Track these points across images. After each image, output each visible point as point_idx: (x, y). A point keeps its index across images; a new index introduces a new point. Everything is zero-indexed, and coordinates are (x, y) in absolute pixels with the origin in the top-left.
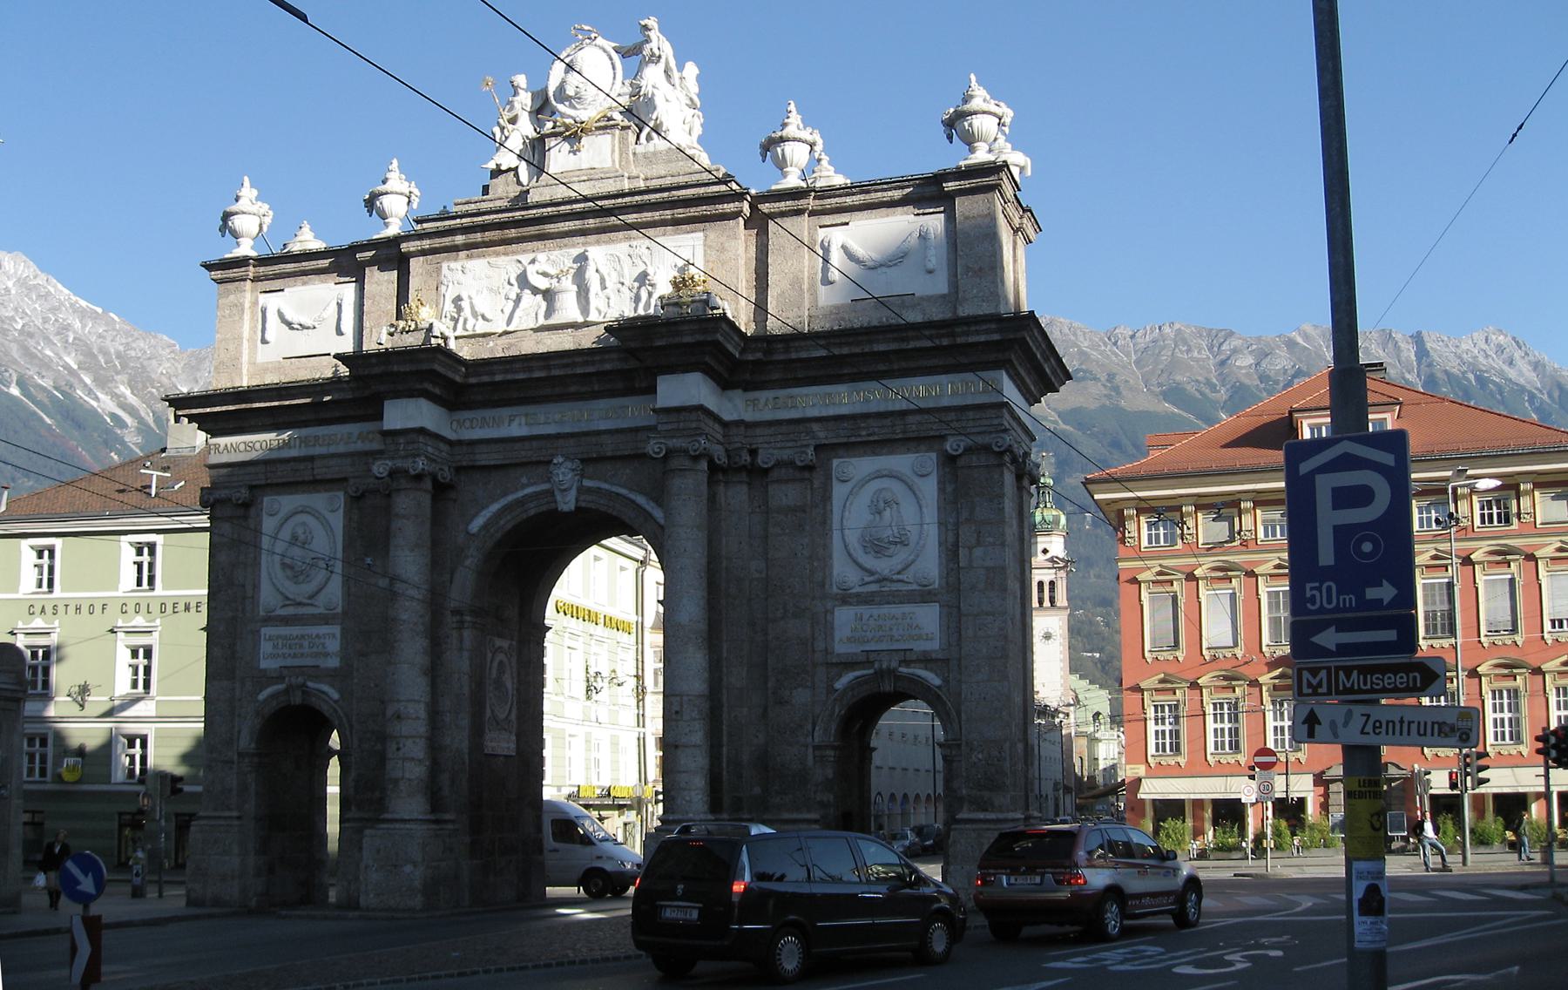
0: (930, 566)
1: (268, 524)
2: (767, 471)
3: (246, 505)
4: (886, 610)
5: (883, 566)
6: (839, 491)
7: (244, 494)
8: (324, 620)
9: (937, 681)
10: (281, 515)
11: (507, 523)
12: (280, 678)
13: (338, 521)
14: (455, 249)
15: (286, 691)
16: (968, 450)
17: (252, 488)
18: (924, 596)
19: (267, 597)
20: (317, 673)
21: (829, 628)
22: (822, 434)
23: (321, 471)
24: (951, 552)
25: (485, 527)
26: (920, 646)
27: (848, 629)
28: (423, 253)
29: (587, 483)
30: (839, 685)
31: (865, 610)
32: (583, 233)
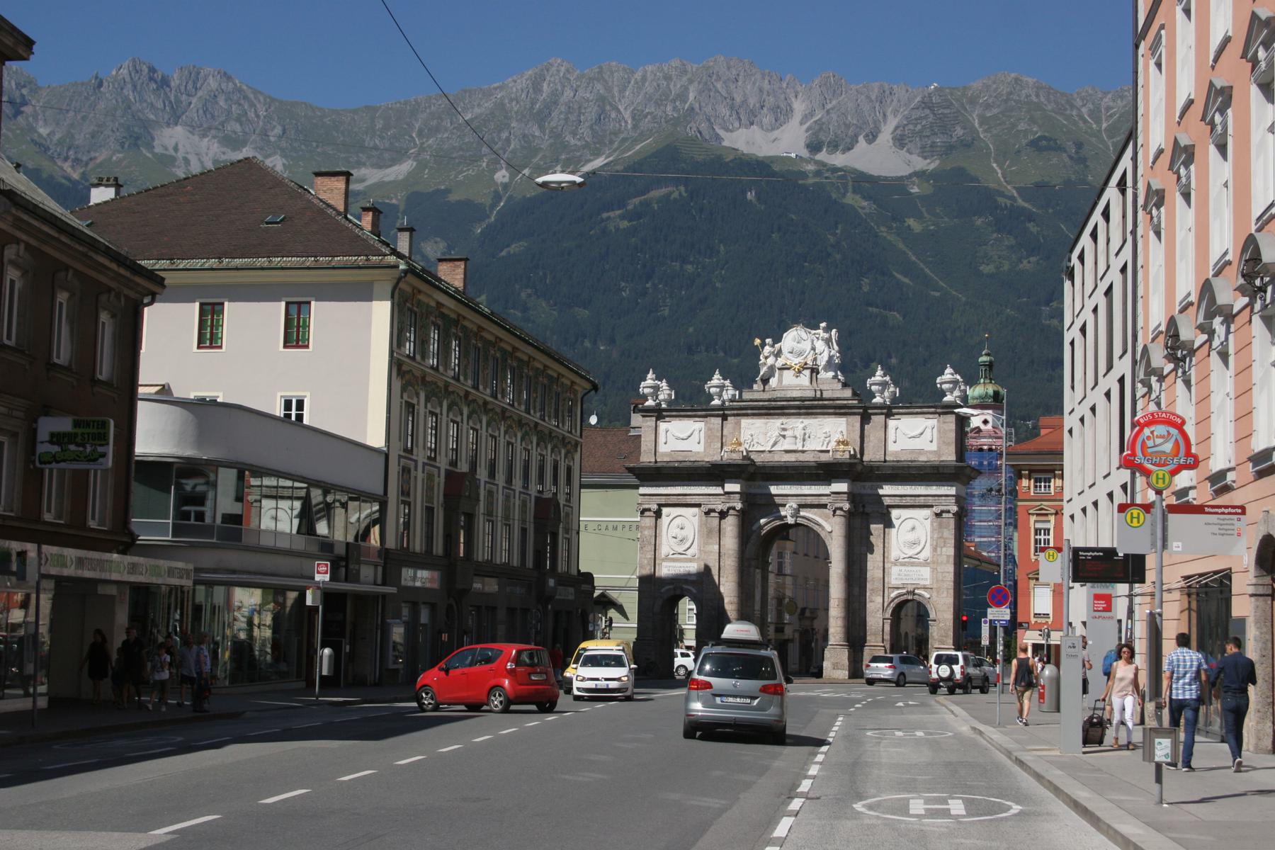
0: (926, 554)
1: (665, 520)
4: (910, 568)
5: (911, 552)
9: (927, 595)
13: (696, 521)
14: (747, 415)
15: (674, 589)
16: (942, 512)
18: (925, 563)
21: (890, 574)
23: (689, 500)
24: (935, 550)
26: (922, 583)
27: (897, 576)
28: (734, 415)
30: (893, 595)
31: (903, 568)
32: (799, 414)
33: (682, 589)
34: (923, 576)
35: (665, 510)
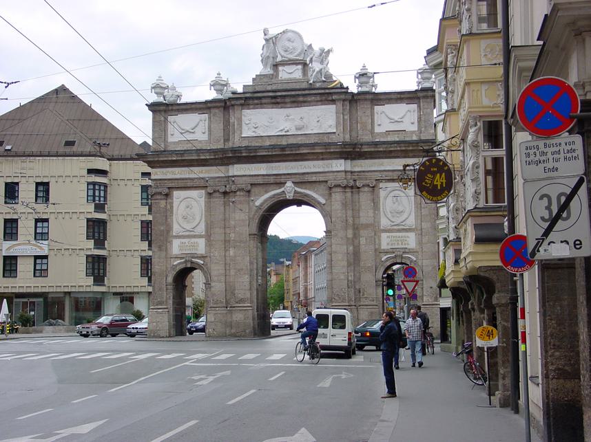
2: (359, 188)
3: (167, 195)
6: (382, 194)
7: (167, 191)
8: (200, 236)
10: (182, 198)
11: (269, 203)
12: (182, 258)
13: (202, 201)
15: (186, 261)
17: (169, 188)
19: (176, 229)
20: (194, 256)
22: (378, 176)
25: (262, 205)
29: (298, 190)
33: (192, 262)
34: (411, 241)
35: (176, 193)
